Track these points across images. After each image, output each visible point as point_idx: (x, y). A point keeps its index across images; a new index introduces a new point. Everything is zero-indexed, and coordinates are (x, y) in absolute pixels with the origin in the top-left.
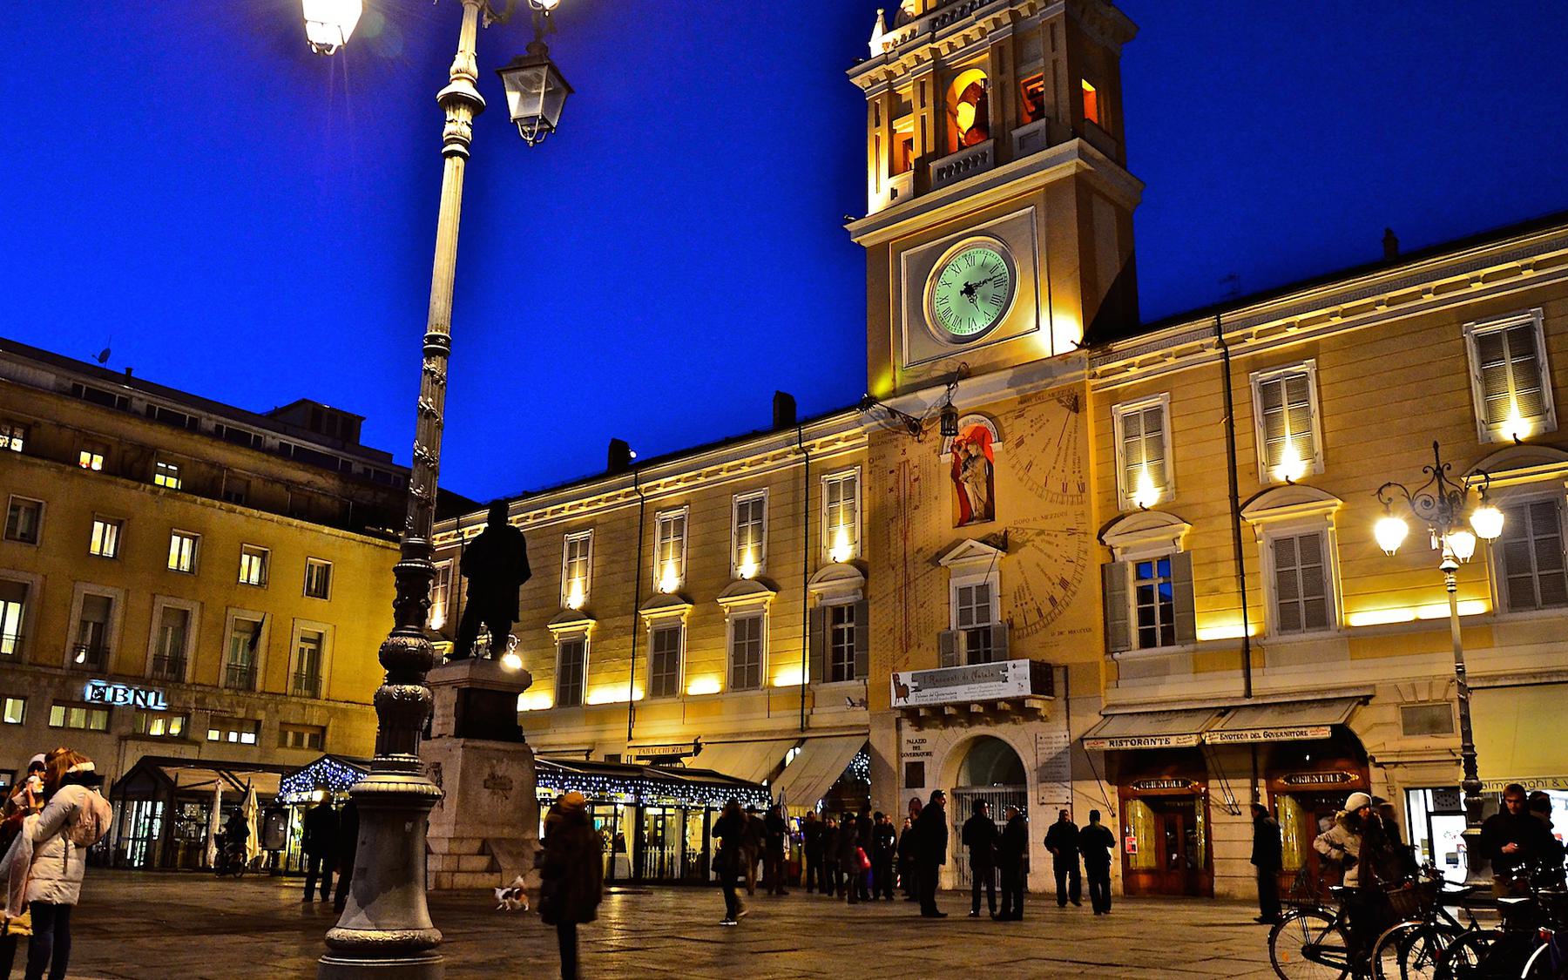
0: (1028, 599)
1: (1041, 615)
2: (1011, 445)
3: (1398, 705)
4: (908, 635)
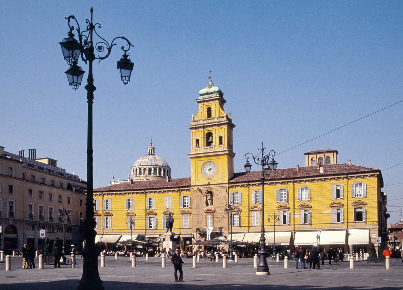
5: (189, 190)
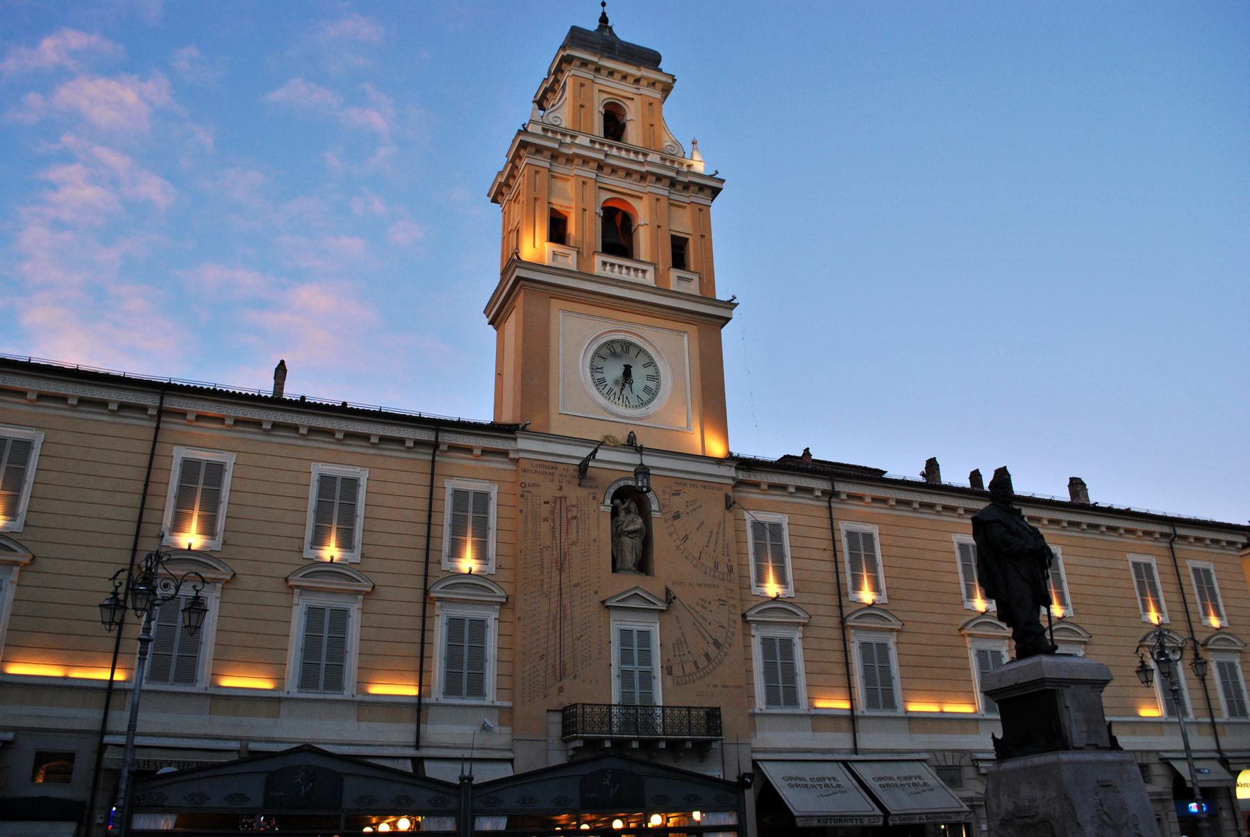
0: (686, 651)
1: (697, 668)
4: (563, 665)
5: (504, 453)
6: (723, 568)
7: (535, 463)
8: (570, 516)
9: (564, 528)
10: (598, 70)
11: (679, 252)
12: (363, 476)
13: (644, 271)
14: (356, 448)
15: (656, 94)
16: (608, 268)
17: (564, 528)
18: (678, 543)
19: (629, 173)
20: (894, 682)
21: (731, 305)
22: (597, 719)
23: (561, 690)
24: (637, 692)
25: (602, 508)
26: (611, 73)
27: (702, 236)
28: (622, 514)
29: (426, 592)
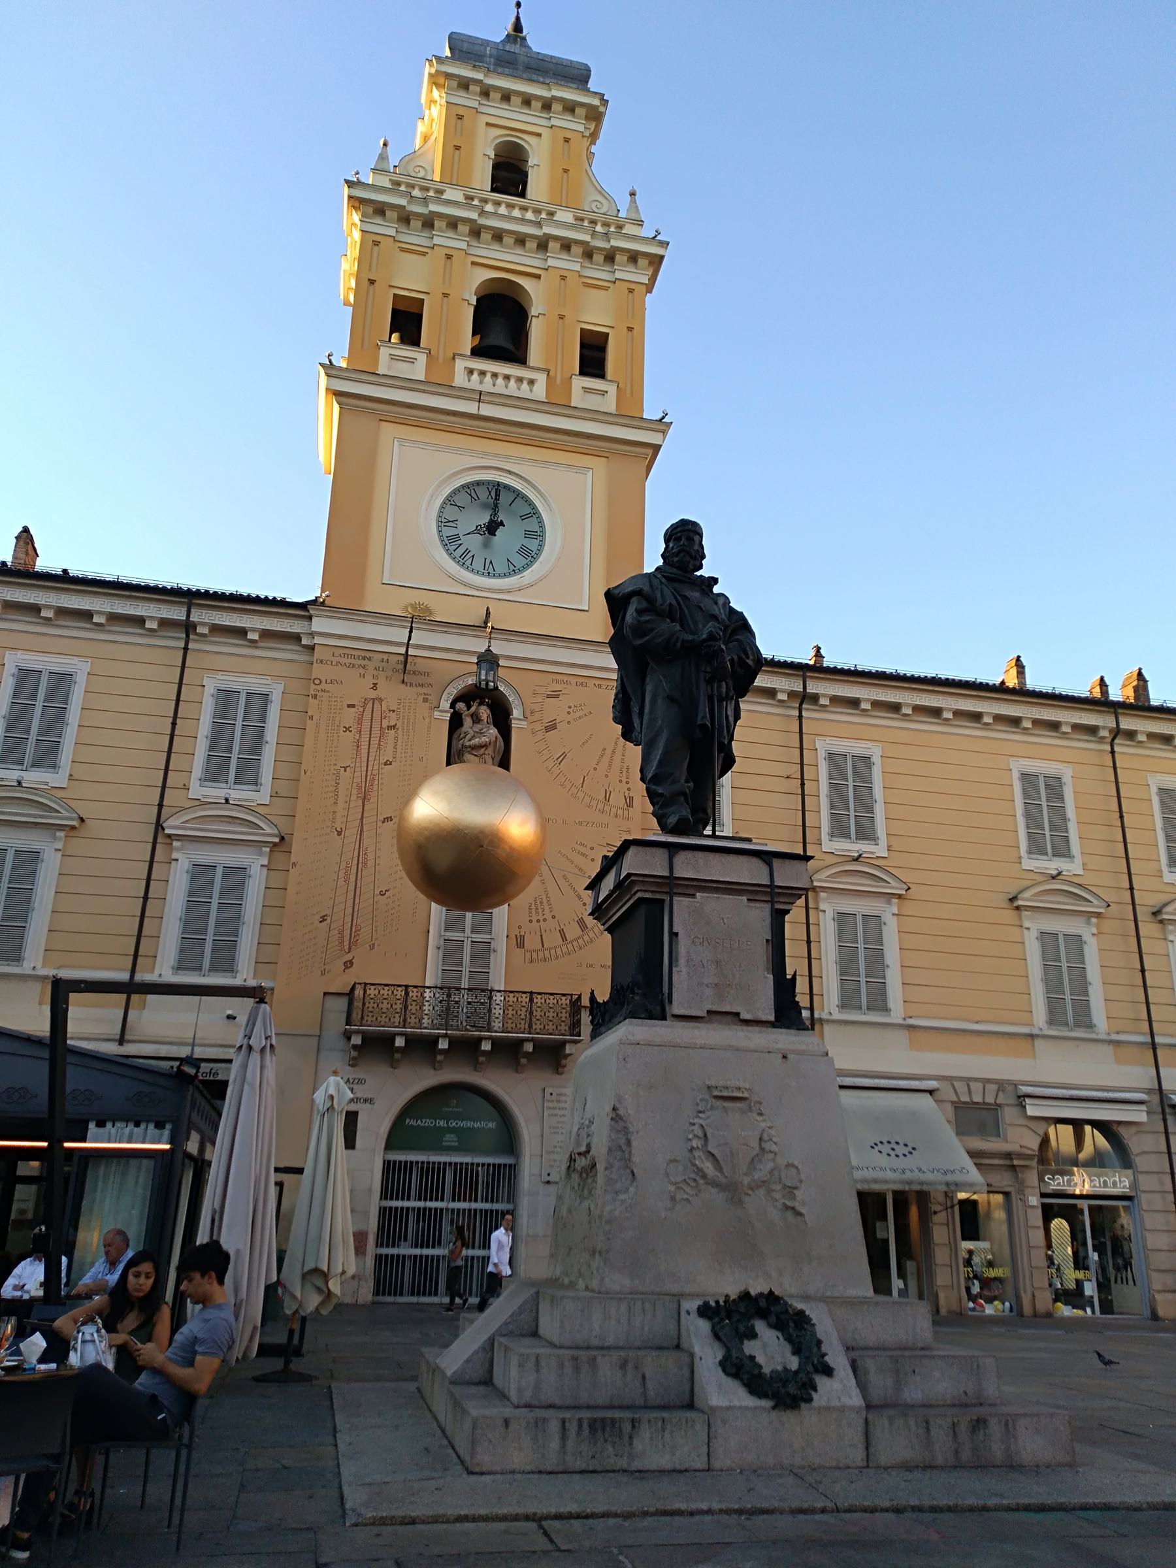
0: (548, 916)
1: (564, 938)
2: (538, 726)
3: (953, 1102)
5: (296, 638)
6: (617, 800)
7: (338, 652)
8: (385, 724)
9: (375, 741)
10: (486, 93)
11: (593, 356)
12: (81, 669)
13: (531, 382)
14: (74, 630)
15: (576, 125)
16: (475, 376)
17: (375, 741)
18: (550, 763)
19: (521, 240)
20: (889, 973)
21: (662, 425)
22: (385, 1006)
23: (349, 964)
24: (466, 970)
25: (437, 714)
26: (506, 97)
27: (630, 329)
28: (468, 722)
29: (159, 826)
